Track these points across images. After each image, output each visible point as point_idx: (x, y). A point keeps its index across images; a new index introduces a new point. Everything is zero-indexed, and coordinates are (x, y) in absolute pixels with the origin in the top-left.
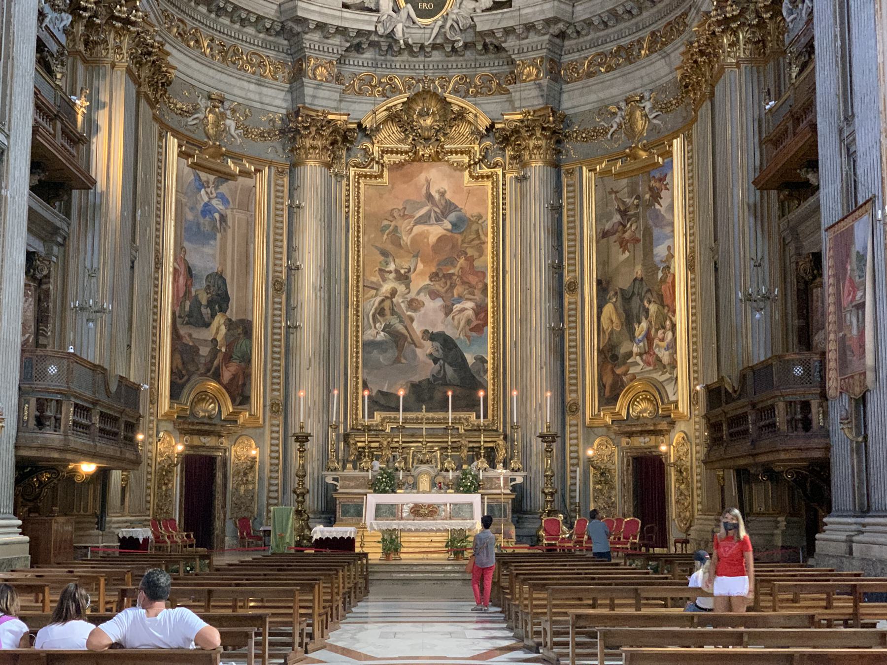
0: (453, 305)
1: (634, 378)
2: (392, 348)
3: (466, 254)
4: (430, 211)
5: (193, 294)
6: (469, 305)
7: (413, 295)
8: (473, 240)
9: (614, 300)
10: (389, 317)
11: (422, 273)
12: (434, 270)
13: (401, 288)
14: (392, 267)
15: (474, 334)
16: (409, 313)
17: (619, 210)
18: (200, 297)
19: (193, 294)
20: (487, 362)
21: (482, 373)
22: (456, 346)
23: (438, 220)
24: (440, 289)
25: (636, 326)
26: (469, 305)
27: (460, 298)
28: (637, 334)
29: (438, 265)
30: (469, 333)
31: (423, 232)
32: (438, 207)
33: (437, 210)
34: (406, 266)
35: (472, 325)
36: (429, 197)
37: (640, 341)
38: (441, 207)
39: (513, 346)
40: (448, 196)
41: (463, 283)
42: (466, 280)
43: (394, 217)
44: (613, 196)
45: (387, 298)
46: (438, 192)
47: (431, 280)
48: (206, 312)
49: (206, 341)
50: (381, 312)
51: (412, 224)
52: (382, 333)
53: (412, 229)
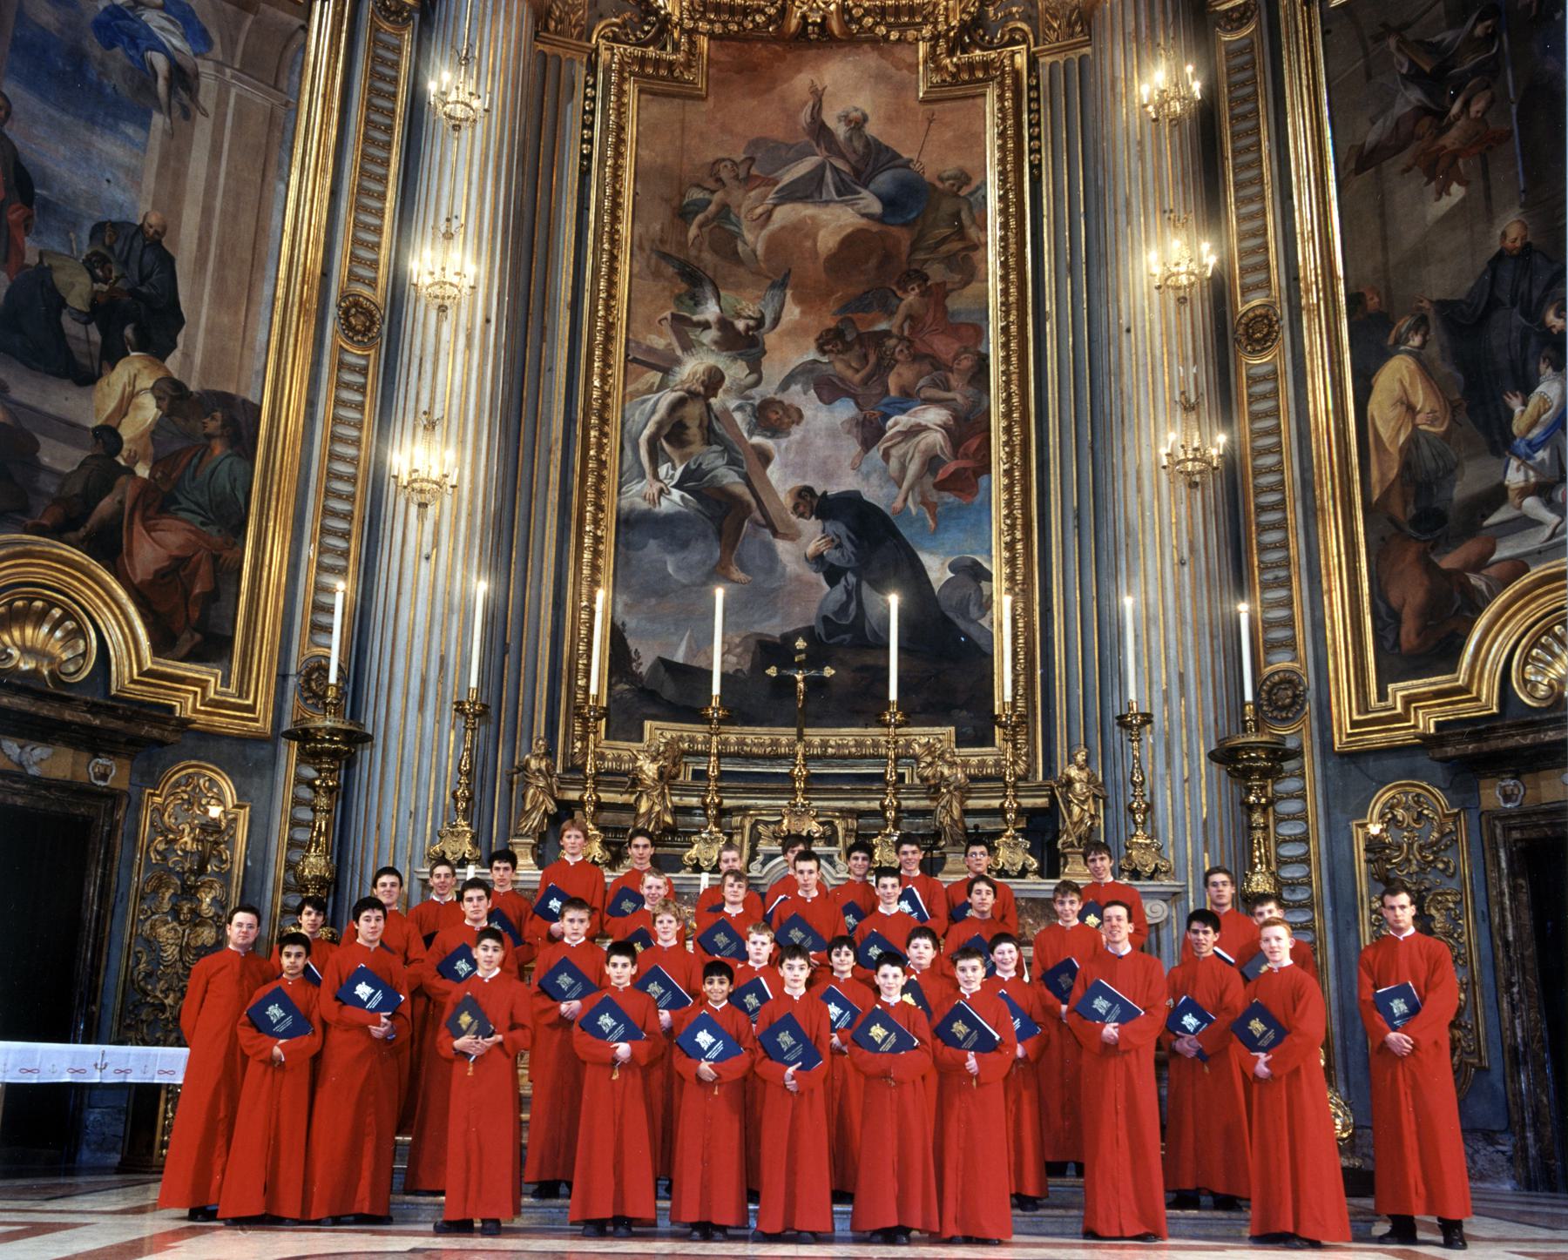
0: (887, 417)
1: (1519, 566)
2: (706, 537)
3: (926, 278)
4: (820, 169)
5: (31, 258)
6: (933, 416)
7: (768, 389)
8: (944, 240)
9: (1416, 341)
10: (697, 448)
11: (796, 331)
12: (830, 323)
13: (735, 371)
14: (711, 311)
15: (949, 498)
16: (756, 440)
17: (1415, 77)
18: (60, 278)
19: (31, 258)
20: (988, 577)
21: (974, 611)
22: (896, 534)
23: (845, 190)
24: (849, 373)
25: (1516, 404)
26: (933, 416)
27: (908, 399)
28: (1518, 426)
29: (844, 308)
30: (934, 496)
31: (802, 221)
32: (842, 156)
33: (840, 164)
34: (751, 309)
35: (942, 474)
36: (819, 130)
37: (1534, 446)
38: (853, 158)
39: (1071, 523)
40: (872, 129)
41: (916, 357)
42: (925, 350)
43: (719, 180)
44: (1392, 42)
45: (692, 395)
46: (846, 118)
47: (821, 349)
48: (84, 336)
49: (73, 425)
50: (673, 432)
51: (769, 201)
52: (676, 494)
53: (769, 215)
